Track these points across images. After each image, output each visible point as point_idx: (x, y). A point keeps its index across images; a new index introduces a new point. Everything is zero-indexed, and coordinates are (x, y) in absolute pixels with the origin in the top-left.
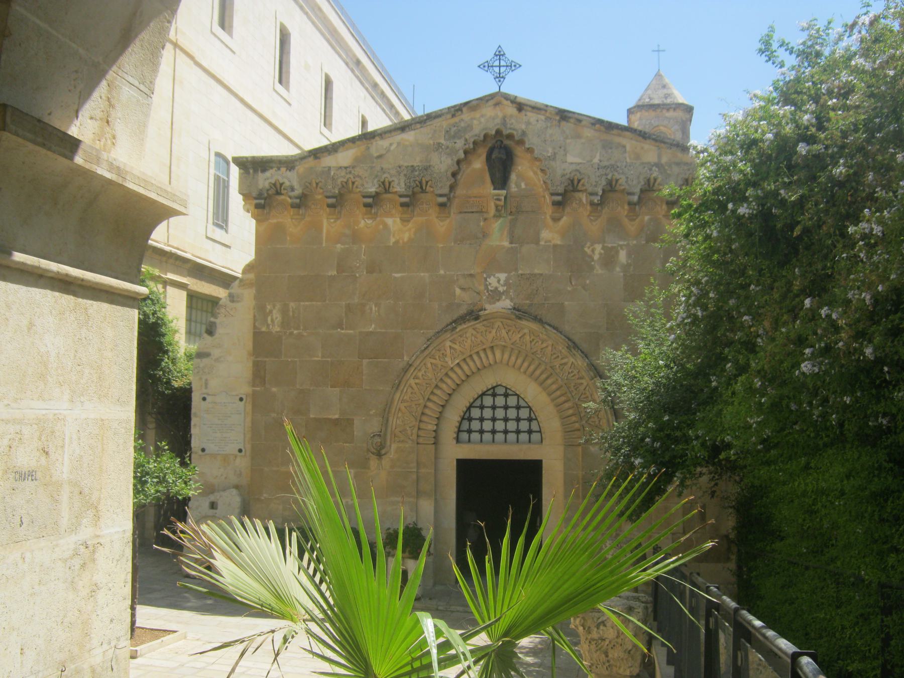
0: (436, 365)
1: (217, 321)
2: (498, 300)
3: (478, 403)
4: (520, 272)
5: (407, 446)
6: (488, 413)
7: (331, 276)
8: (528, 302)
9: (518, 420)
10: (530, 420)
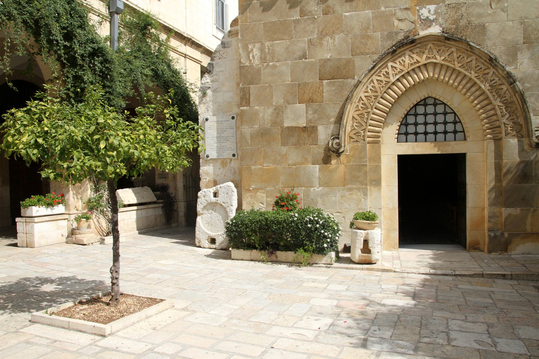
0: (381, 81)
1: (214, 62)
2: (430, 27)
3: (413, 112)
4: (447, 3)
5: (360, 145)
6: (421, 119)
7: (296, 20)
8: (454, 26)
9: (445, 123)
10: (455, 123)
